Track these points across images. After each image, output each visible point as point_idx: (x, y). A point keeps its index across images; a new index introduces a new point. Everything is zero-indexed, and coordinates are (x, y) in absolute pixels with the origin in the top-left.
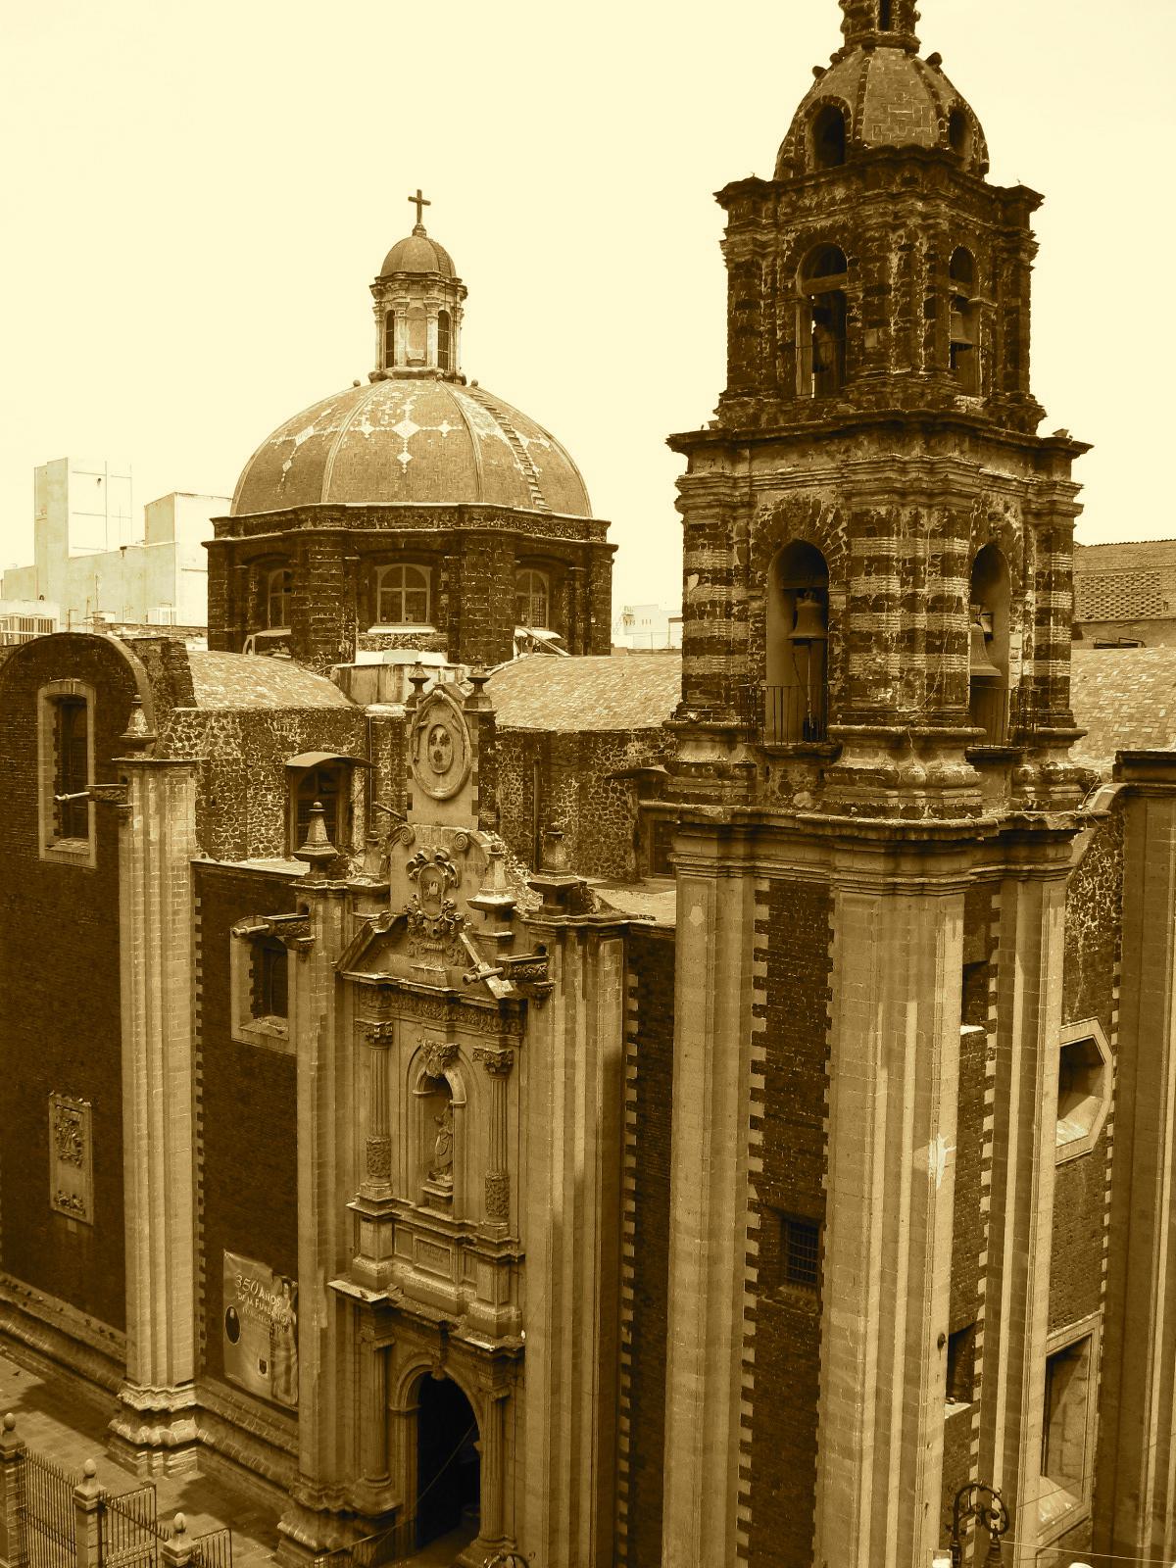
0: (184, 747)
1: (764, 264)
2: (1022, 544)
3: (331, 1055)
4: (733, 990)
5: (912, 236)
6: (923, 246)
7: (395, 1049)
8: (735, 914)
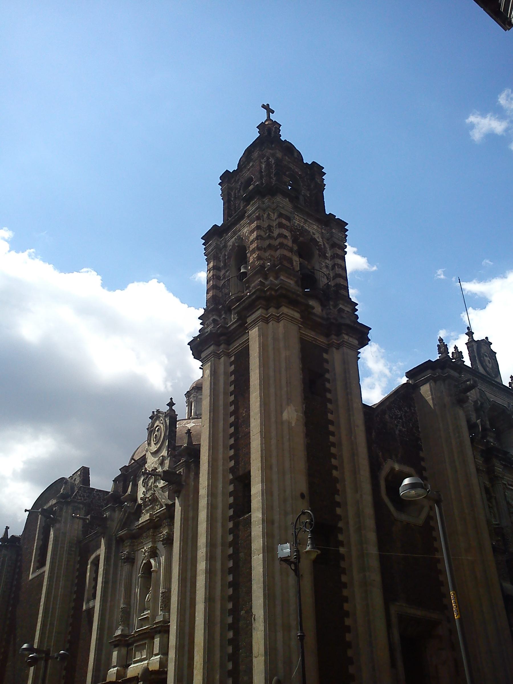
0: (81, 499)
1: (232, 194)
2: (323, 247)
3: (111, 577)
4: (221, 397)
5: (268, 159)
6: (272, 160)
7: (135, 565)
8: (221, 369)
